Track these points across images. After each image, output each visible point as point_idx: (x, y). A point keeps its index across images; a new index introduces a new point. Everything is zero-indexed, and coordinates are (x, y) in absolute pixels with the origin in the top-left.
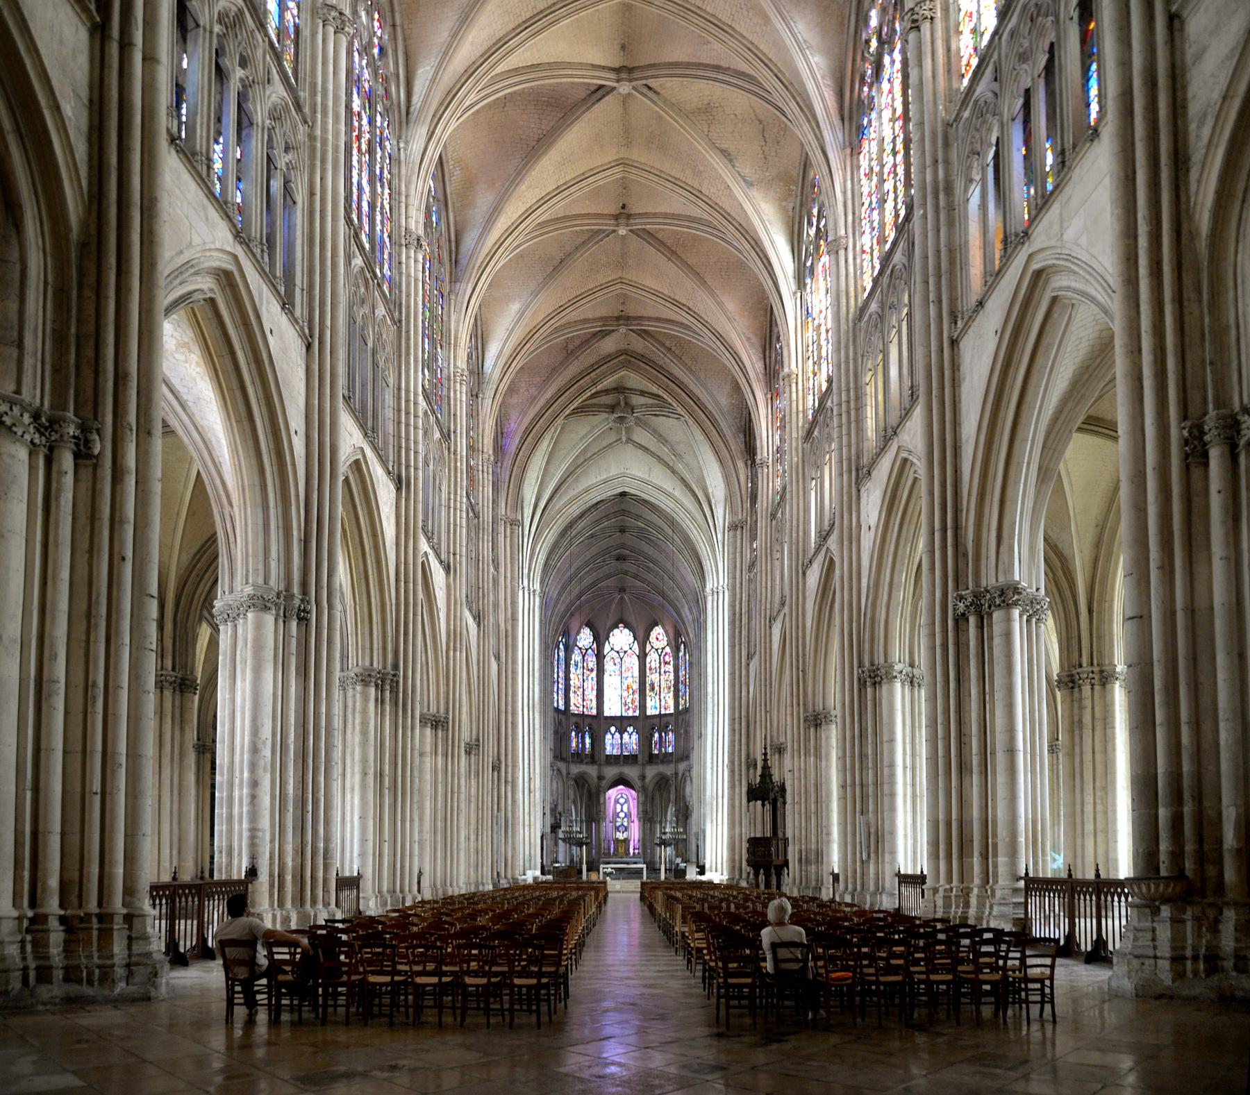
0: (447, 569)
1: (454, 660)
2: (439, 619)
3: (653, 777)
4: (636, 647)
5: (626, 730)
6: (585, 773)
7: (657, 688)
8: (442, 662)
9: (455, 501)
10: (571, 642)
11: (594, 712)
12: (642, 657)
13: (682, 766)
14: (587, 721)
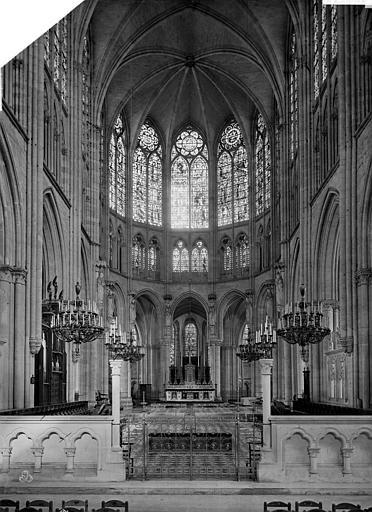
5: (194, 245)
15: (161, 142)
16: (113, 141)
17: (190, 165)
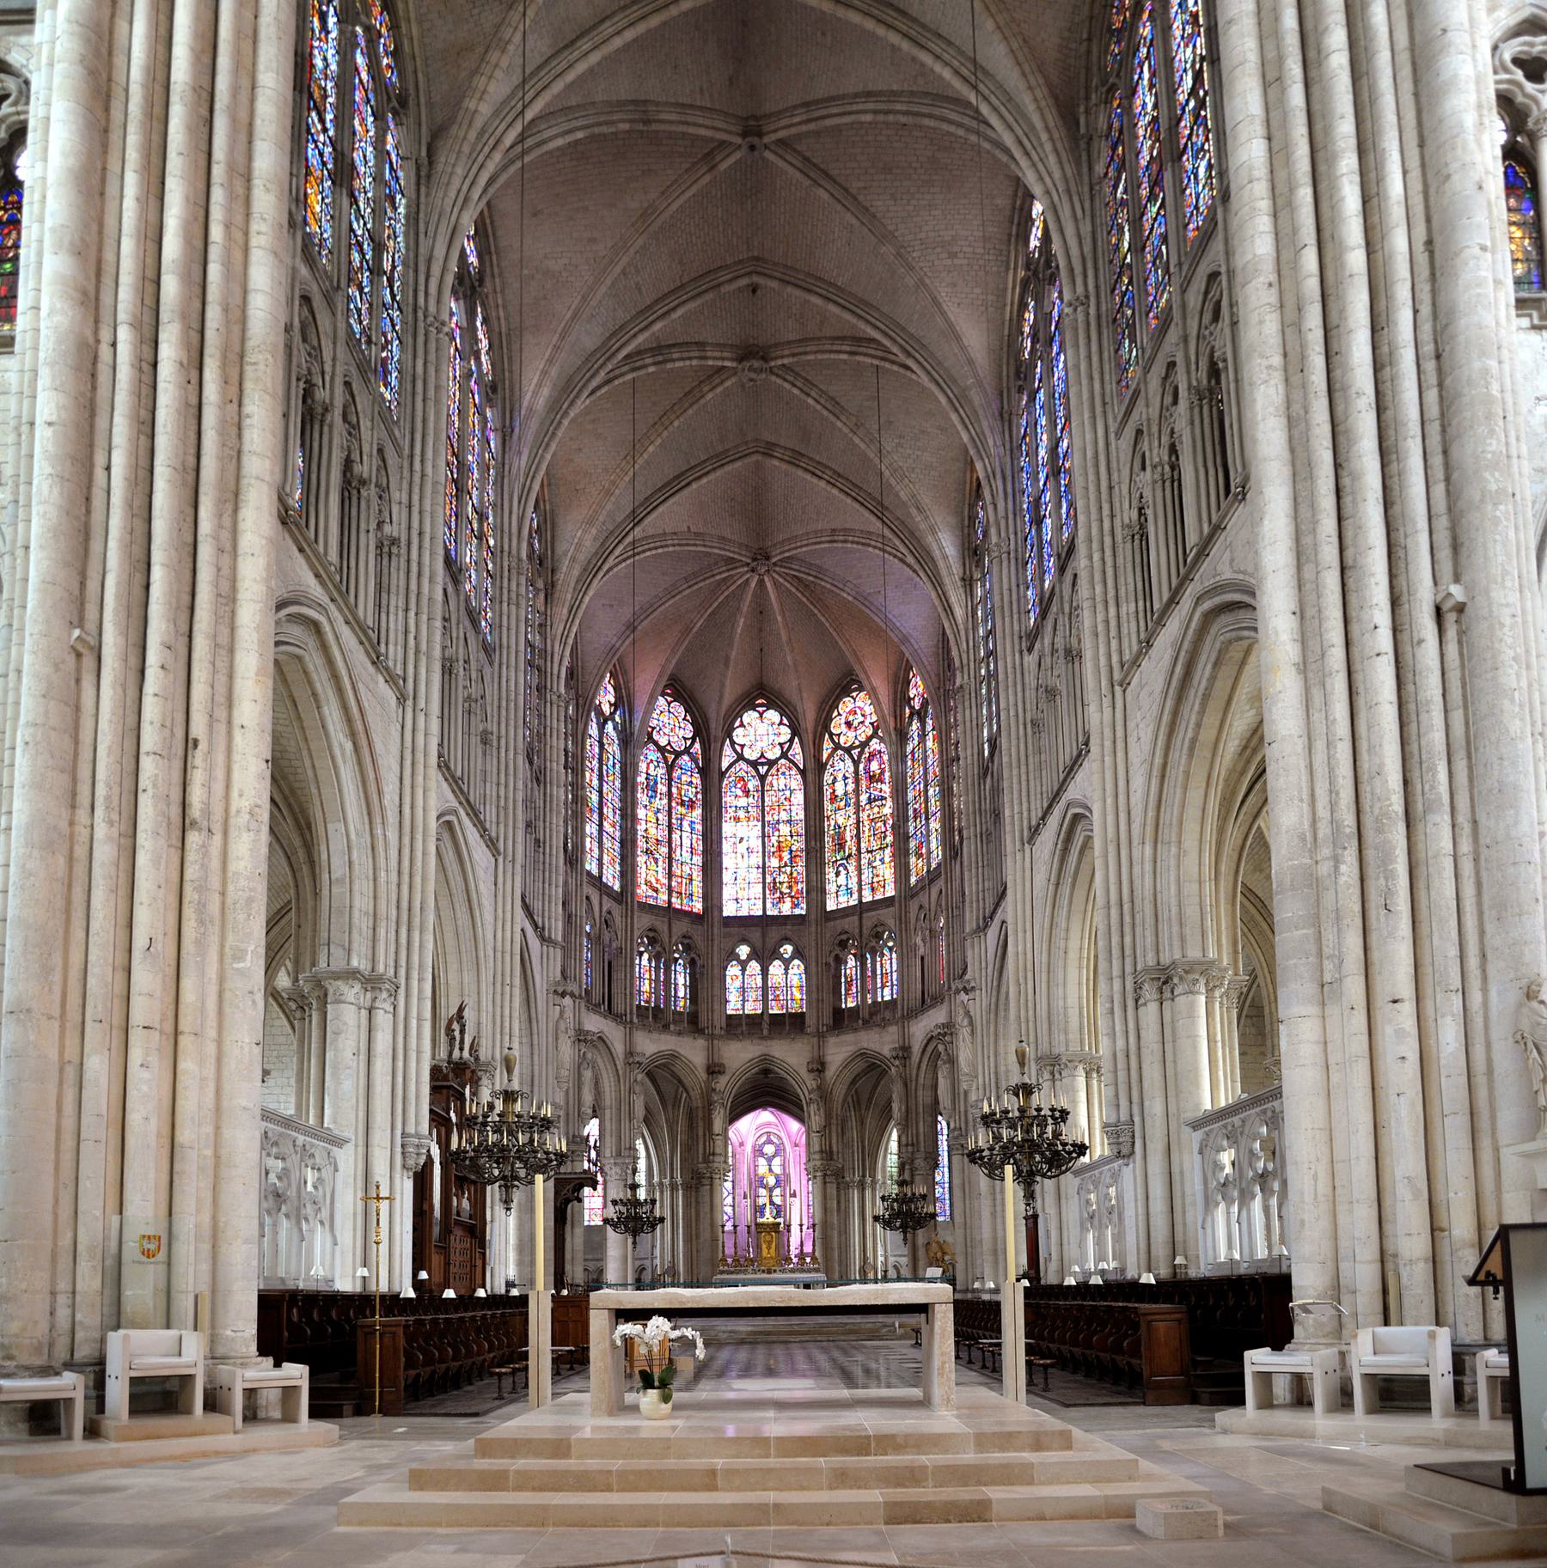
4: (797, 747)
5: (775, 954)
6: (674, 1056)
7: (850, 845)
11: (698, 906)
13: (921, 1029)
14: (680, 927)
15: (701, 730)
16: (593, 730)
17: (762, 778)
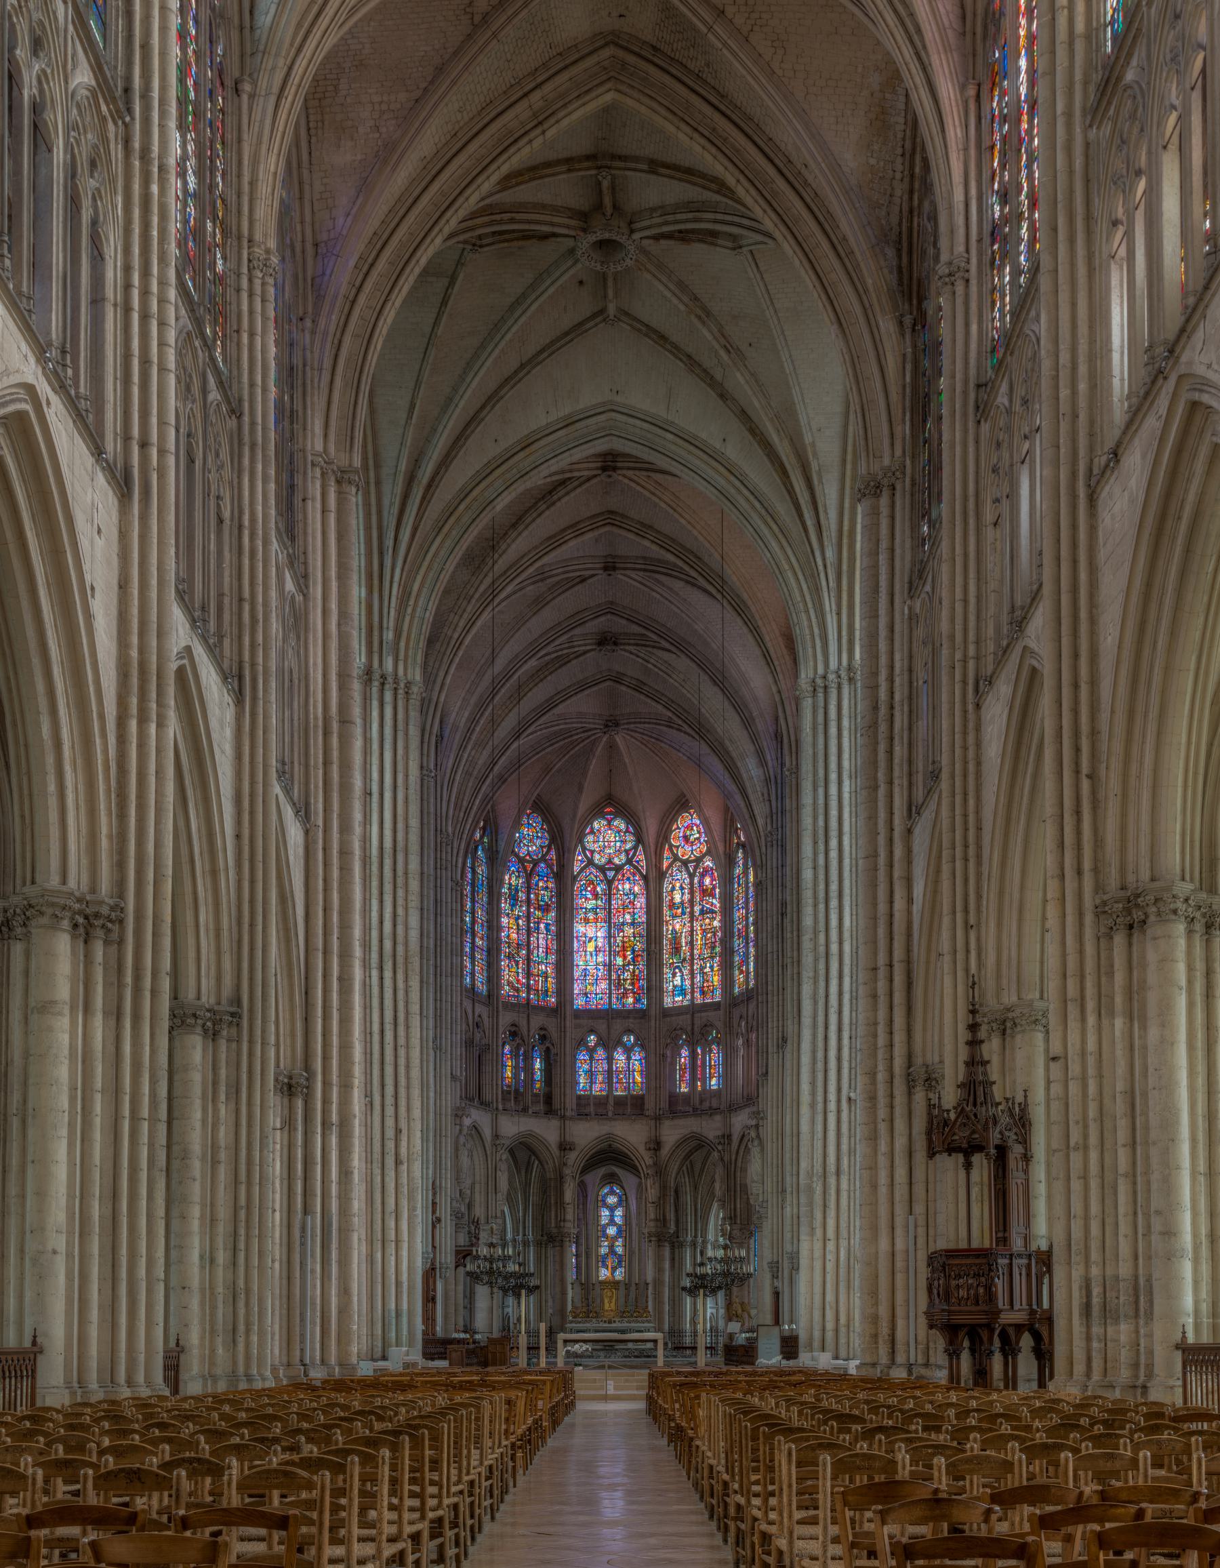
0: (122, 482)
1: (142, 745)
2: (89, 616)
3: (679, 1145)
4: (640, 856)
5: (619, 1043)
8: (105, 747)
9: (145, 293)
10: (502, 845)
12: (654, 880)
17: (610, 883)
